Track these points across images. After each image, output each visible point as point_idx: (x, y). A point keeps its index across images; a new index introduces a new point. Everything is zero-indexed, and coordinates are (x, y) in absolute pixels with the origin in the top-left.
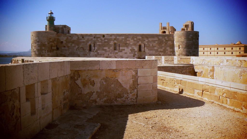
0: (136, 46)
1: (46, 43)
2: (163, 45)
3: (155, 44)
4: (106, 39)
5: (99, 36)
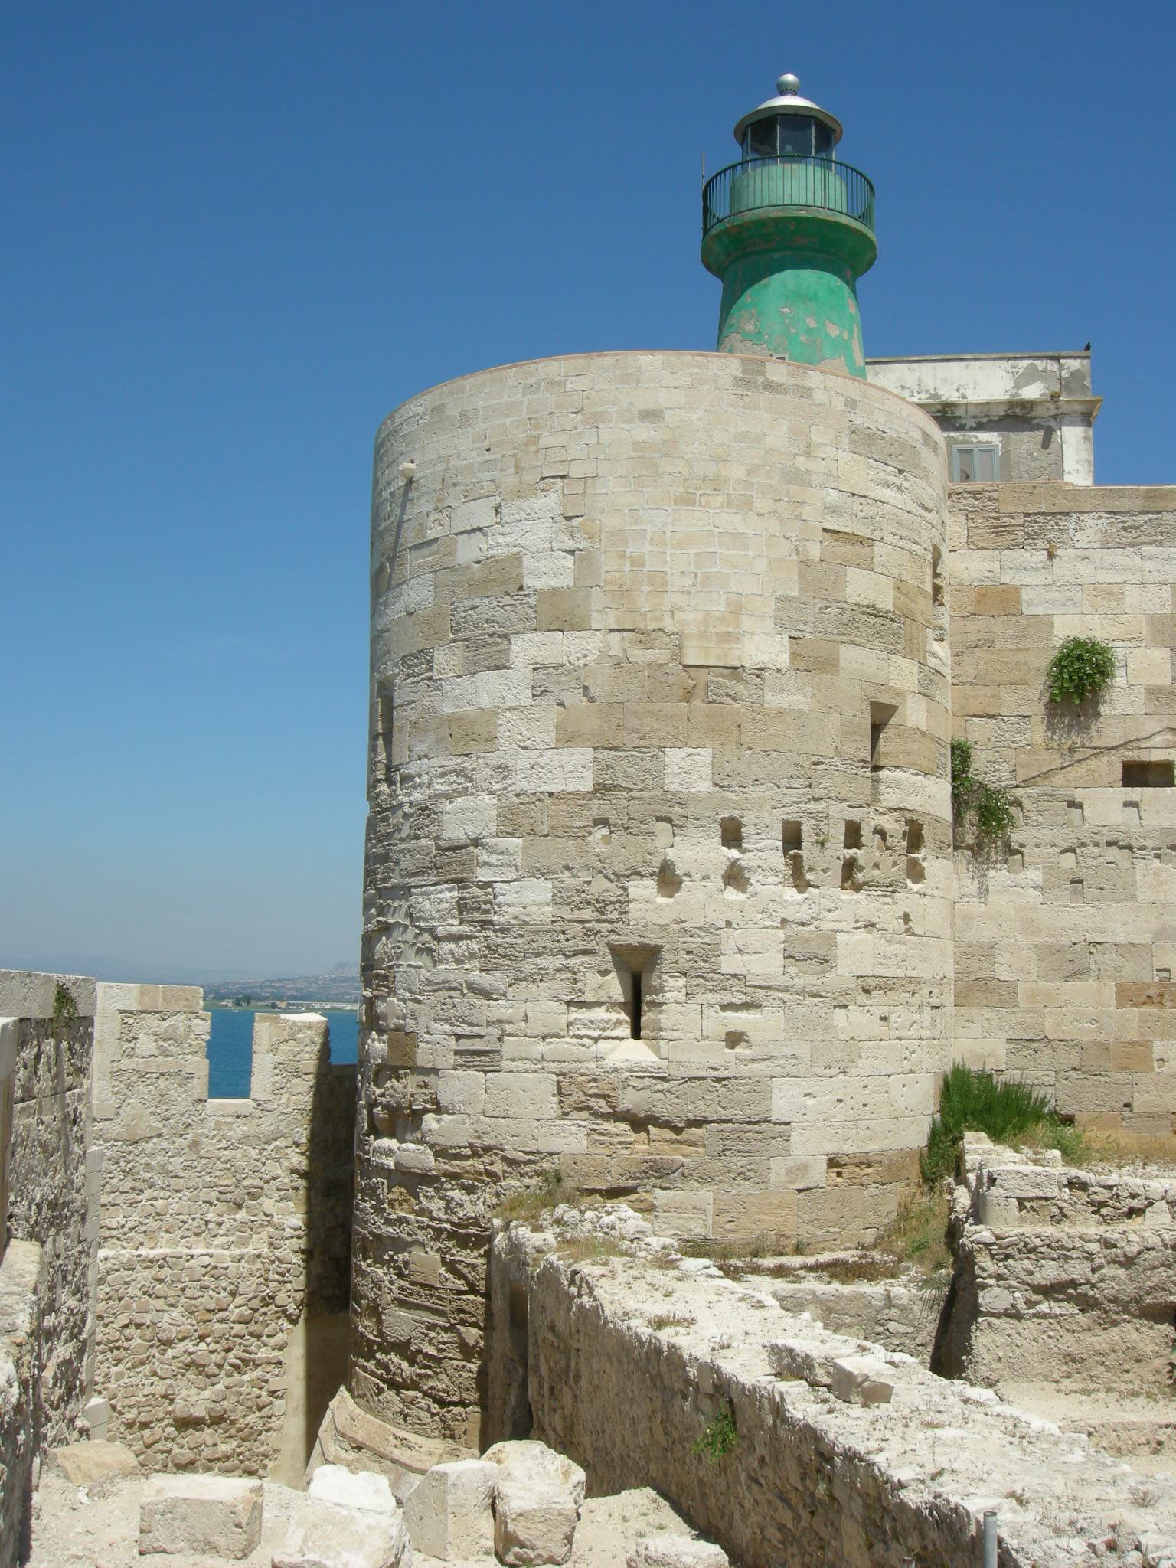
1: (766, 648)
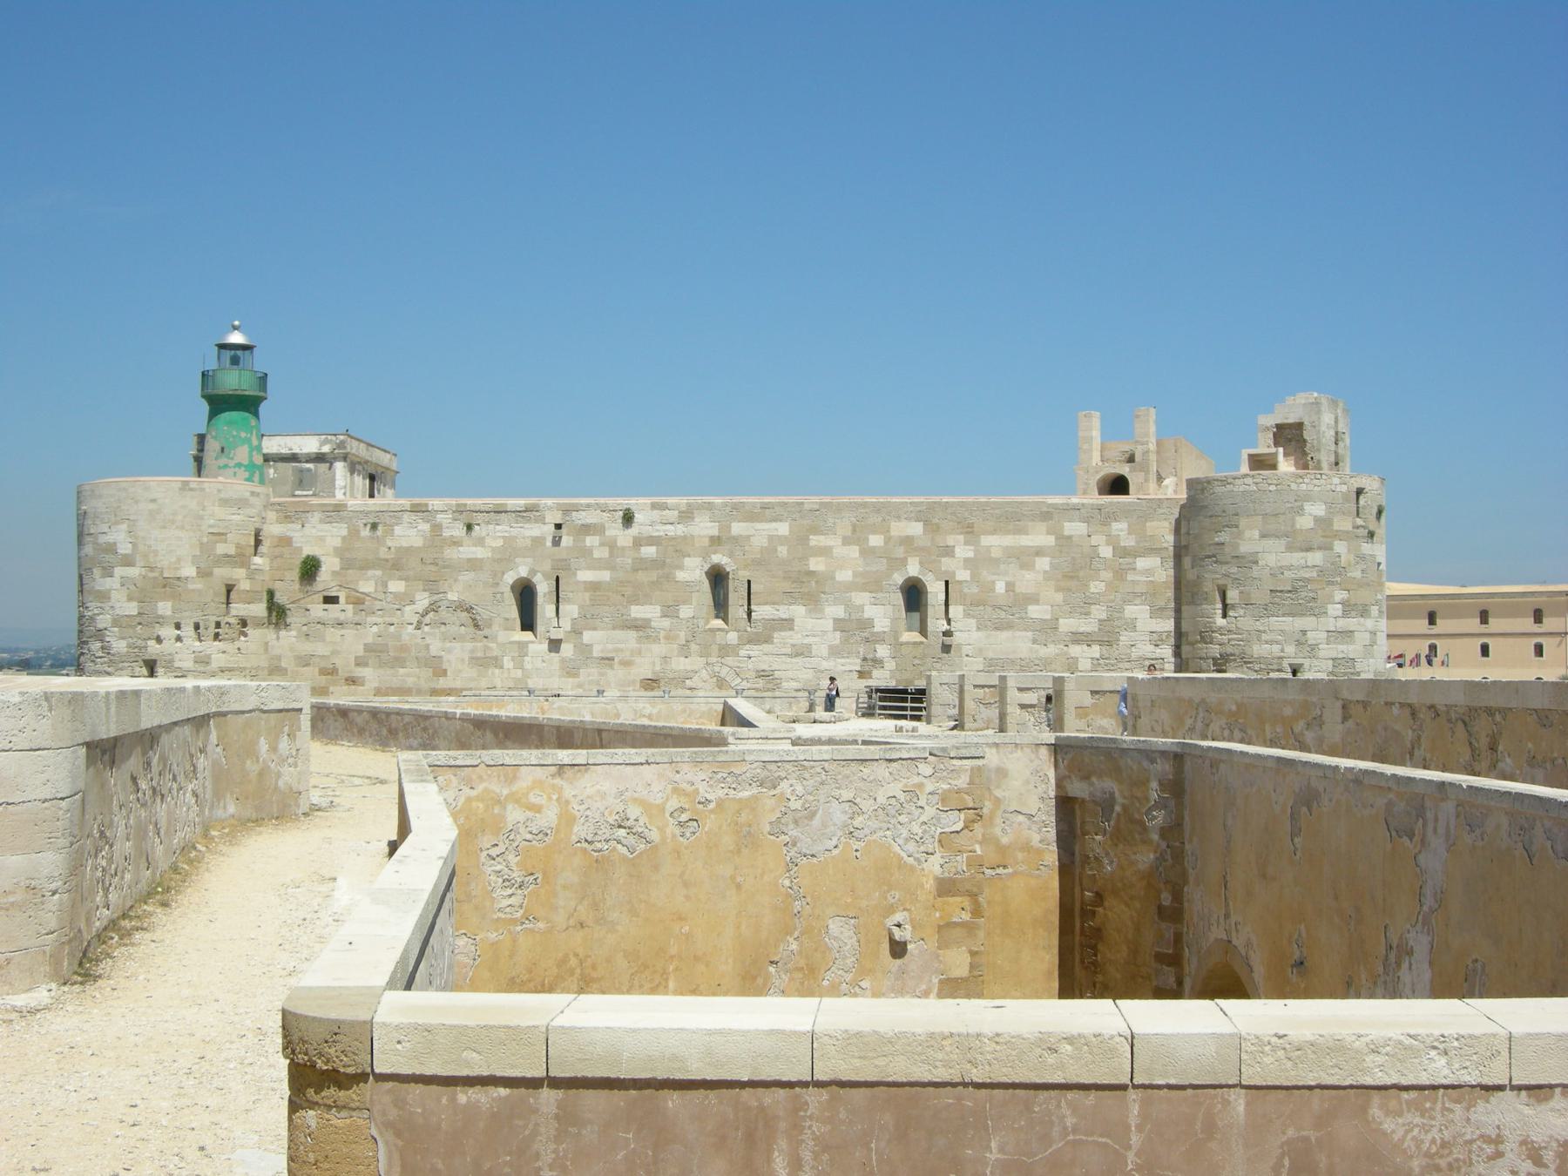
0: (880, 595)
1: (189, 571)
2: (1096, 587)
3: (1027, 581)
4: (652, 541)
5: (589, 521)
